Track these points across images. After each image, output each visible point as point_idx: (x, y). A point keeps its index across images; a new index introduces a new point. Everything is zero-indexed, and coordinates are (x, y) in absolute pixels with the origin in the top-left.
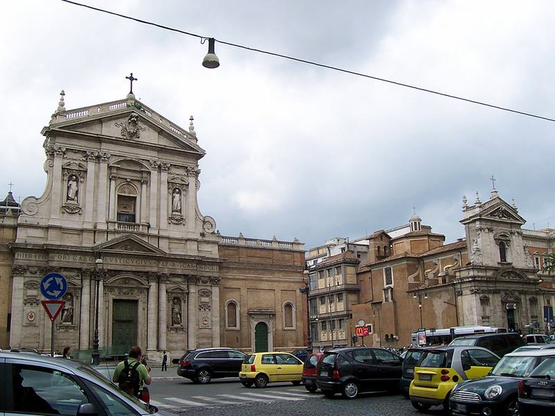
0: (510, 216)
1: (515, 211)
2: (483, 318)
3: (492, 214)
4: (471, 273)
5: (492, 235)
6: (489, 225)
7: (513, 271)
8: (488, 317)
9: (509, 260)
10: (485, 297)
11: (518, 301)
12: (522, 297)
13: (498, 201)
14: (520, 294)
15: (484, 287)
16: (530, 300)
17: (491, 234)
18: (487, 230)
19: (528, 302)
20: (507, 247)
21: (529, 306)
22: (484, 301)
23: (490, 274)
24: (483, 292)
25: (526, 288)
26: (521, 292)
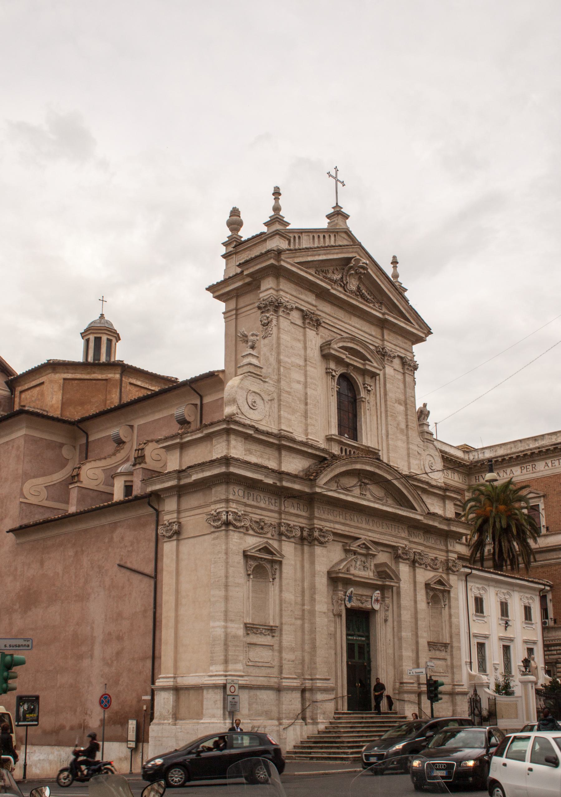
0: (381, 298)
1: (400, 291)
2: (249, 628)
3: (321, 267)
4: (219, 449)
5: (315, 339)
6: (308, 301)
7: (374, 474)
8: (272, 630)
9: (368, 438)
10: (266, 550)
11: (385, 583)
12: (404, 569)
13: (343, 241)
14: (397, 558)
15: (265, 510)
16: (427, 586)
17: (311, 333)
18: (296, 316)
19: (422, 595)
20: (363, 394)
21: (422, 605)
22: (261, 565)
23: (294, 465)
24: (259, 528)
25: (416, 544)
26: (397, 555)
